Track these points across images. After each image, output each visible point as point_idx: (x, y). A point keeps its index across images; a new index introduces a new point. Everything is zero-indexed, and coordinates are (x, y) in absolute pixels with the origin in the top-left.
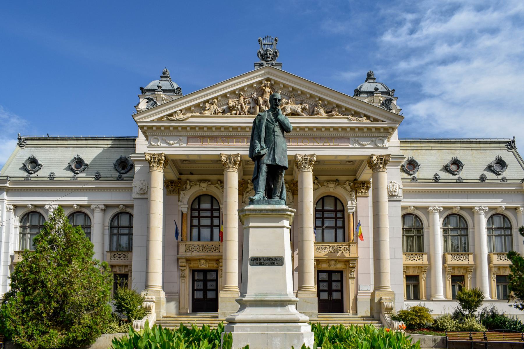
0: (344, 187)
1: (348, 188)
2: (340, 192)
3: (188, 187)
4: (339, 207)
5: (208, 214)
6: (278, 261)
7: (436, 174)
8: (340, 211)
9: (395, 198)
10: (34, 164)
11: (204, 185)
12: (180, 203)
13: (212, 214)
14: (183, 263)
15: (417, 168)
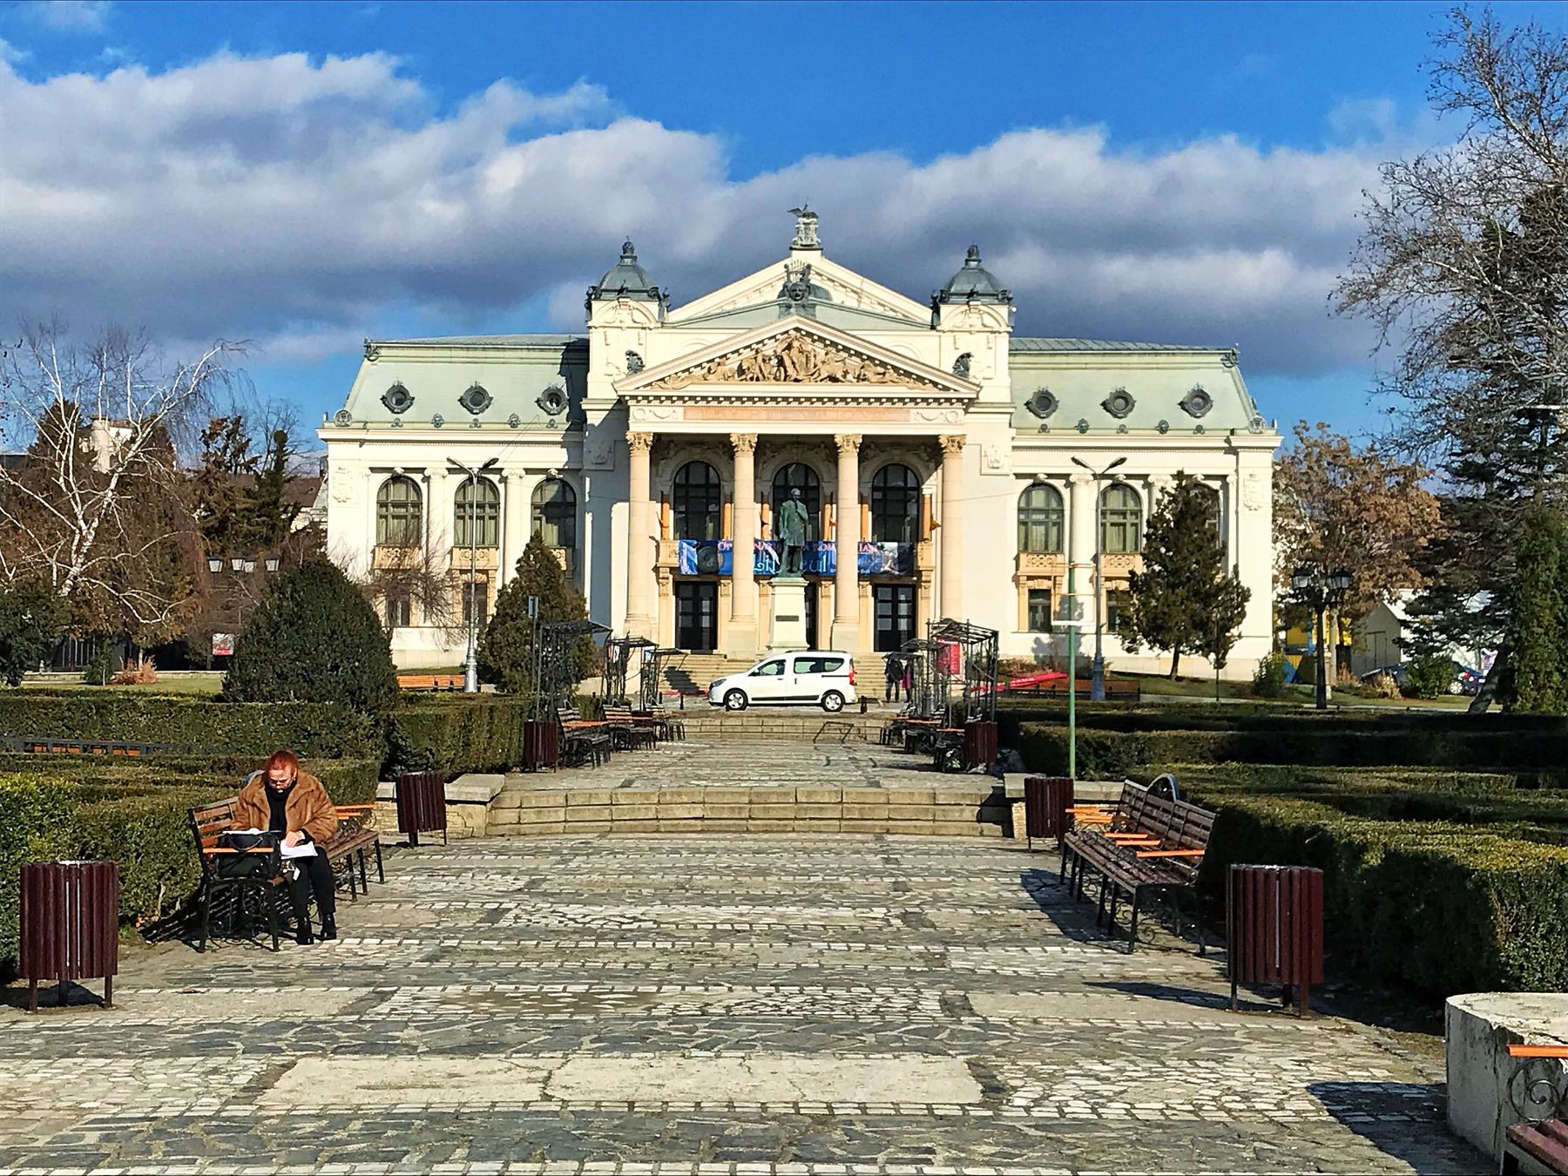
0: (919, 457)
1: (924, 455)
2: (911, 459)
3: (672, 453)
4: (911, 483)
5: (702, 493)
6: (795, 618)
7: (1083, 421)
8: (913, 489)
9: (995, 471)
10: (400, 396)
11: (697, 450)
12: (658, 479)
13: (707, 492)
14: (665, 572)
15: (1053, 407)
